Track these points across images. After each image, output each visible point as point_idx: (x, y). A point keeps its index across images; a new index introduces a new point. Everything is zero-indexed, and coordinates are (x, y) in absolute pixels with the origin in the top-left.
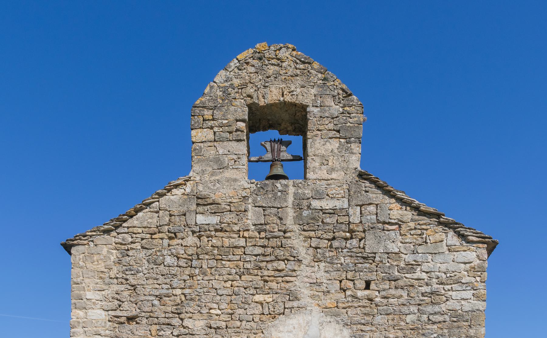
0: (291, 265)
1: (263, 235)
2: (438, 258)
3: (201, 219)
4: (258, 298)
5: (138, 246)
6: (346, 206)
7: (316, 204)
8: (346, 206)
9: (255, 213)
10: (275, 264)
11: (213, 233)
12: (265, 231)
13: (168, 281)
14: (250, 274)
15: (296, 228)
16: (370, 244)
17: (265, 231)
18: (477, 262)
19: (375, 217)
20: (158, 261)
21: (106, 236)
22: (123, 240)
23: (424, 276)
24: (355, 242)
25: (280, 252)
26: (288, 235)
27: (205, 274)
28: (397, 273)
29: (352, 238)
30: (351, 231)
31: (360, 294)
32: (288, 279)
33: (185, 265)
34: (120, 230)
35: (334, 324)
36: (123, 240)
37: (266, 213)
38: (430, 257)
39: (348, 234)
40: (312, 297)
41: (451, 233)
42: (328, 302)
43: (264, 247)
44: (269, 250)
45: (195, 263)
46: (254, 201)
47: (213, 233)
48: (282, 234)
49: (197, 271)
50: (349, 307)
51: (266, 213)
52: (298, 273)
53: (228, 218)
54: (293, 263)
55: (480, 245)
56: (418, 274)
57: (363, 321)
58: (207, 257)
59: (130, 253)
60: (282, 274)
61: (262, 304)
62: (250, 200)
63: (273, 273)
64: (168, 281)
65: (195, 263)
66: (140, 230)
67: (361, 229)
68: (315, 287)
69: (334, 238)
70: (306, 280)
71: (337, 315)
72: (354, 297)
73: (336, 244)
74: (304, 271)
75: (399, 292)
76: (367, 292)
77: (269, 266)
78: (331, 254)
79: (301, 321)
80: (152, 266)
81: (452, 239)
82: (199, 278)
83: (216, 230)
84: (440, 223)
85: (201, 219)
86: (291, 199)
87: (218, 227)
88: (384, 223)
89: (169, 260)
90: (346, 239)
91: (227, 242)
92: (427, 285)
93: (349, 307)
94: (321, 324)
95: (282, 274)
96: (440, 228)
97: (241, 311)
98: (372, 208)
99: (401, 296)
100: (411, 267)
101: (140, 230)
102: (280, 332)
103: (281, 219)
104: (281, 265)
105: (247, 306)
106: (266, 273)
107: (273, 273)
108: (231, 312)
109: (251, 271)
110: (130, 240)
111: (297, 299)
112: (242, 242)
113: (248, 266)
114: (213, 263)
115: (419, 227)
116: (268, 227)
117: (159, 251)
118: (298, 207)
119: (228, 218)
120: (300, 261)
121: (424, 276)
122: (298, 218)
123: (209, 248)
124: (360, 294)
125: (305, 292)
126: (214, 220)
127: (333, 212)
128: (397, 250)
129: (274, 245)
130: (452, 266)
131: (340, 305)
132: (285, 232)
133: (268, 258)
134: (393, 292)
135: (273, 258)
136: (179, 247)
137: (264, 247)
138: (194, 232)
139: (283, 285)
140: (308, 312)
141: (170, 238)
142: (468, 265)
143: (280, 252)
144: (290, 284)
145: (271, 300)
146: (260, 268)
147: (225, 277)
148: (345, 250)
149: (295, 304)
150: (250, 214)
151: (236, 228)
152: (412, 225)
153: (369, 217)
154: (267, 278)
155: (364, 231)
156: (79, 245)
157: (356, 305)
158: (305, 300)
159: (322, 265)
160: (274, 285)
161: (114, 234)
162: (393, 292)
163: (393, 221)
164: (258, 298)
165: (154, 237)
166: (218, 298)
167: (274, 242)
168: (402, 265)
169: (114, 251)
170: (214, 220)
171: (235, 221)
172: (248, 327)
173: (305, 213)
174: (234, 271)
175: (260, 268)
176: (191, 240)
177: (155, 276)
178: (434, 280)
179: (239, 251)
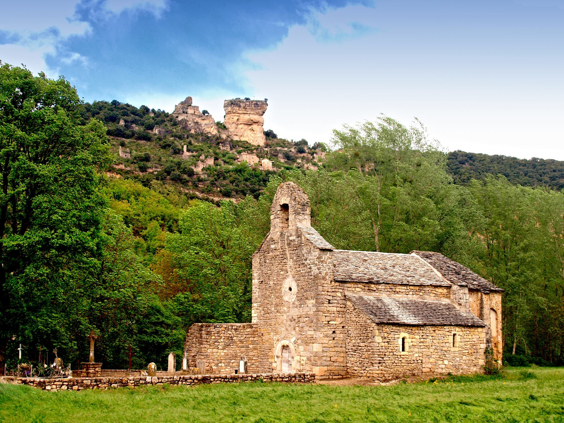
15: (287, 247)
86: (286, 237)
124: (298, 269)
125: (289, 270)
149: (287, 274)
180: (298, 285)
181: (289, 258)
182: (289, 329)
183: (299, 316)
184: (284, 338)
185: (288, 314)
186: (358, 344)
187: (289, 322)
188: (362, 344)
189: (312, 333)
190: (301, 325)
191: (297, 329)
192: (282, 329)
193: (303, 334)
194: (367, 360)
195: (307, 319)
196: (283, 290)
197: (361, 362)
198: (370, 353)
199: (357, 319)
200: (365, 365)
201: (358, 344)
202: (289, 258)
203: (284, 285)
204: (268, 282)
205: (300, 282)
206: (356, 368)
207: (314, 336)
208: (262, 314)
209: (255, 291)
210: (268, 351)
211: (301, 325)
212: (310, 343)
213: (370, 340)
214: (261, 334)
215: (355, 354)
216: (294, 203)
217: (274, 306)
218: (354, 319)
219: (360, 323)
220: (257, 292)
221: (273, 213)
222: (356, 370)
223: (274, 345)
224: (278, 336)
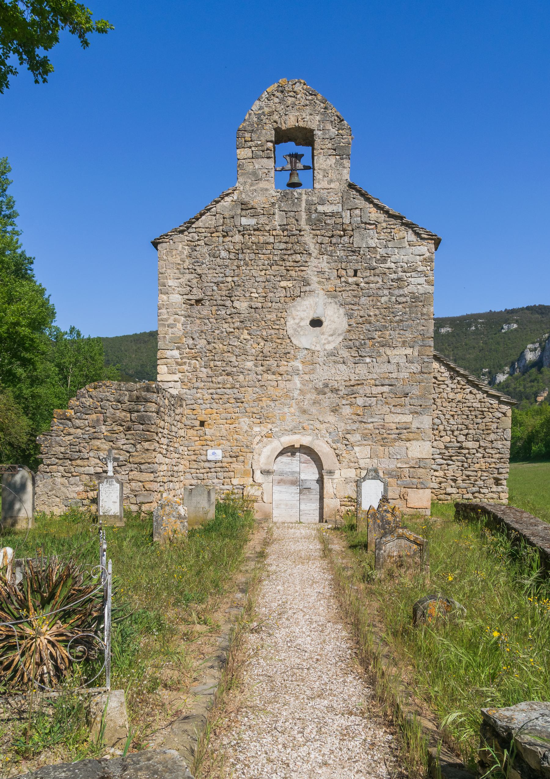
0: (305, 257)
1: (286, 233)
2: (402, 252)
3: (245, 221)
4: (283, 284)
5: (202, 243)
6: (340, 210)
7: (320, 208)
8: (340, 210)
9: (280, 216)
10: (294, 257)
11: (252, 232)
12: (287, 230)
13: (222, 270)
14: (277, 265)
15: (307, 228)
16: (357, 241)
17: (287, 230)
18: (427, 255)
19: (359, 219)
20: (216, 255)
21: (181, 235)
22: (192, 238)
23: (393, 265)
24: (346, 239)
25: (297, 247)
26: (302, 233)
27: (247, 265)
28: (375, 264)
29: (344, 236)
30: (344, 230)
31: (351, 280)
32: (302, 268)
33: (234, 258)
34: (191, 230)
35: (333, 304)
36: (192, 238)
37: (288, 216)
38: (396, 250)
39: (342, 233)
40: (319, 283)
41: (410, 232)
42: (329, 287)
43: (286, 243)
44: (290, 245)
45: (241, 256)
46: (280, 207)
47: (252, 232)
48: (298, 232)
49: (242, 262)
50: (344, 291)
51: (288, 216)
52: (309, 264)
53: (263, 220)
54: (305, 256)
55: (430, 241)
56: (389, 264)
57: (353, 302)
58: (249, 251)
59: (198, 248)
60: (298, 264)
61: (285, 289)
62: (277, 206)
63: (292, 264)
64: (222, 270)
65: (241, 256)
66: (203, 230)
67: (350, 228)
68: (321, 275)
69: (333, 236)
70: (315, 269)
71: (335, 297)
72: (346, 282)
73: (334, 240)
74: (313, 262)
75: (377, 279)
76: (355, 279)
77: (290, 258)
78: (331, 248)
79: (312, 302)
80: (212, 259)
81: (410, 236)
82: (244, 268)
83: (255, 230)
84: (403, 224)
85: (245, 221)
86: (303, 204)
87: (256, 227)
88: (366, 223)
89: (224, 254)
90: (341, 236)
91: (262, 239)
92: (395, 272)
93: (344, 291)
94: (325, 304)
95: (298, 264)
96: (403, 228)
97: (271, 295)
98: (357, 212)
99: (378, 282)
100: (384, 259)
101: (203, 230)
102: (298, 311)
103: (297, 220)
104: (298, 257)
105: (275, 291)
106: (288, 264)
107: (292, 264)
108: (265, 295)
109: (278, 262)
110: (197, 238)
111: (309, 284)
112: (271, 240)
113: (276, 258)
114: (252, 256)
115: (389, 226)
116: (288, 227)
117: (217, 247)
118: (309, 211)
119: (263, 220)
120: (310, 254)
121: (393, 265)
122: (309, 220)
123: (250, 244)
124: (351, 280)
125: (314, 279)
126: (252, 222)
127: (332, 215)
128: (374, 245)
129: (293, 241)
130: (411, 258)
131: (338, 289)
132: (300, 231)
133: (289, 252)
134: (372, 278)
135: (292, 252)
136: (230, 243)
137: (286, 243)
138: (239, 231)
139: (299, 273)
140: (316, 295)
141: (224, 236)
142: (422, 257)
143: (297, 247)
144: (304, 273)
145: (291, 285)
146: (284, 260)
147: (261, 267)
148: (340, 246)
149: (307, 288)
150: (277, 217)
151: (267, 228)
152: (384, 225)
153: (355, 219)
154: (288, 268)
155: (353, 230)
156: (163, 242)
157: (348, 289)
158: (314, 286)
159: (325, 257)
160: (293, 273)
161: (186, 233)
162: (372, 278)
163: (371, 222)
164: (283, 284)
165: (213, 235)
166: (257, 284)
167: (293, 240)
168: (378, 257)
169: (186, 247)
170: (252, 222)
171: (267, 222)
172: (277, 307)
173: (314, 216)
174: (266, 262)
175: (284, 260)
176: (238, 238)
177: (214, 266)
178: (400, 269)
179: (270, 247)
180: (350, 316)
181: (315, 253)
182: (314, 410)
183: (352, 383)
184: (293, 431)
185: (306, 377)
186: (459, 445)
187: (313, 396)
188: (470, 444)
189: (408, 418)
190: (360, 401)
191: (347, 411)
192: (286, 410)
193: (370, 420)
194: (485, 474)
195: (386, 389)
196: (291, 323)
197: (464, 477)
198: (493, 460)
199: (459, 397)
200: (480, 483)
201: (459, 445)
202: (315, 253)
203: (294, 313)
204: (228, 303)
205: (355, 307)
206: (449, 490)
207: (414, 426)
208: (203, 375)
209: (171, 321)
210: (230, 460)
211: (360, 401)
212: (395, 440)
213: (492, 437)
214: (198, 423)
215: (451, 463)
216: (333, 131)
217: (250, 358)
218: (451, 396)
219: (469, 404)
220: (179, 326)
221: (250, 144)
222: (449, 494)
223: (254, 446)
224: (270, 426)
